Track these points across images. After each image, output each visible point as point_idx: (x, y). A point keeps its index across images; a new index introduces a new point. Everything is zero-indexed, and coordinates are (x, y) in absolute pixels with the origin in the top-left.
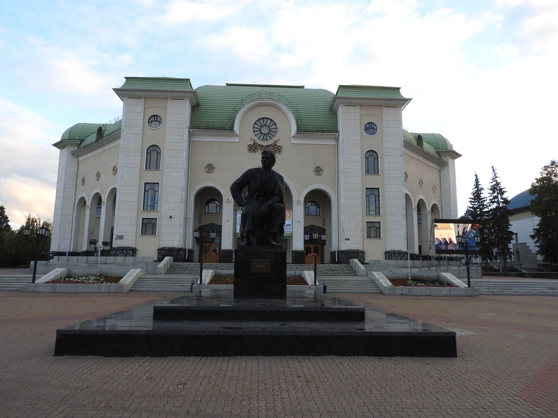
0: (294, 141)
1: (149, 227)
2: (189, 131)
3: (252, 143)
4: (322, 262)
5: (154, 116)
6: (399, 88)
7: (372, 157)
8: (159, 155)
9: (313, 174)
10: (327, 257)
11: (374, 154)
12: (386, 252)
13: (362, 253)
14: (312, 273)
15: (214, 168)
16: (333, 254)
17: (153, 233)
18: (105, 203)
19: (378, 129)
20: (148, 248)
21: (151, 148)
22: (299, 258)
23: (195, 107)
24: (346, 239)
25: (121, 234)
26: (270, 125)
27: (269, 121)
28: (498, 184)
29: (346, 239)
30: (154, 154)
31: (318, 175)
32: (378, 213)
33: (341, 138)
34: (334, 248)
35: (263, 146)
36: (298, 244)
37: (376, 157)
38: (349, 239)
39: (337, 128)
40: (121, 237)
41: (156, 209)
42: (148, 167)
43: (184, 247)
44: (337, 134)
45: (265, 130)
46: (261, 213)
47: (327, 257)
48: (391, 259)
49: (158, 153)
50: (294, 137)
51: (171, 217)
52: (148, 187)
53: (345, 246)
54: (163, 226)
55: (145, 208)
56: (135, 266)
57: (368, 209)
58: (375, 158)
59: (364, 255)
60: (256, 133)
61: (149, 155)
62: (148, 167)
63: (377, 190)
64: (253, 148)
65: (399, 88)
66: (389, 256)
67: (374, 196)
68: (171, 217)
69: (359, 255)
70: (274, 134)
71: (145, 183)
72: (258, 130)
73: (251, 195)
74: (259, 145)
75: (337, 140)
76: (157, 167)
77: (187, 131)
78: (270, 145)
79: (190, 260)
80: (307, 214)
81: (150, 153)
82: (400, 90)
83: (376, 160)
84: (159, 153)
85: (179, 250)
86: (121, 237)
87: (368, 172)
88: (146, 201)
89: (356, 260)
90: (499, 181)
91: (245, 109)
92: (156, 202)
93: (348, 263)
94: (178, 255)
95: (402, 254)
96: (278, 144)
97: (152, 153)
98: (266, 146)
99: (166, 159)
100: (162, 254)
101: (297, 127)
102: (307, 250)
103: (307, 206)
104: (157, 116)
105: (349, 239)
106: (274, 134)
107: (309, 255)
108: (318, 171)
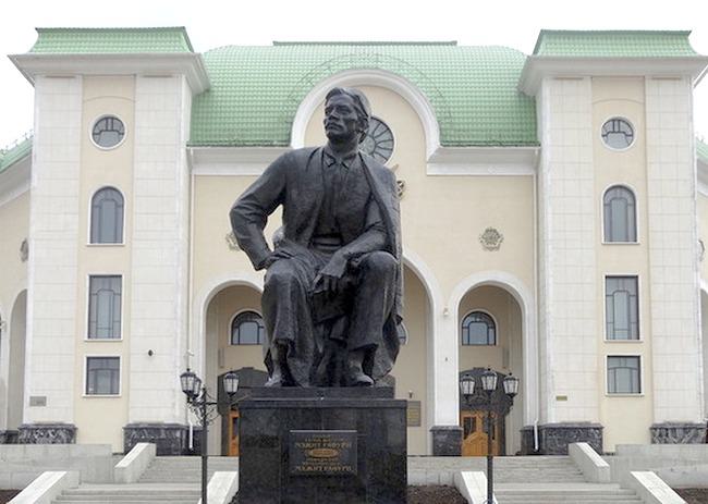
0: (433, 170)
1: (102, 374)
2: (188, 151)
4: (502, 453)
5: (106, 118)
6: (688, 33)
7: (622, 204)
10: (514, 440)
11: (625, 194)
12: (654, 428)
13: (595, 429)
14: (482, 477)
16: (528, 433)
19: (636, 133)
20: (101, 423)
21: (102, 195)
22: (448, 444)
23: (202, 97)
24: (558, 398)
25: (40, 394)
26: (377, 133)
29: (558, 398)
30: (109, 207)
31: (491, 249)
32: (634, 333)
33: (548, 155)
34: (531, 420)
36: (446, 411)
37: (630, 201)
38: (565, 398)
39: (536, 135)
40: (39, 402)
42: (96, 238)
43: (183, 423)
44: (537, 148)
46: (321, 282)
47: (514, 440)
48: (666, 442)
50: (432, 161)
51: (150, 353)
52: (98, 284)
53: (556, 416)
54: (132, 374)
57: (610, 326)
58: (627, 205)
59: (600, 434)
61: (97, 210)
62: (96, 238)
63: (633, 281)
65: (688, 33)
66: (660, 435)
67: (625, 295)
68: (150, 353)
69: (590, 433)
70: (385, 153)
71: (91, 277)
73: (293, 230)
75: (536, 163)
76: (117, 238)
77: (183, 151)
80: (466, 341)
82: (689, 37)
83: (630, 209)
84: (119, 206)
85: (172, 428)
86: (39, 402)
87: (610, 237)
88: (93, 319)
89: (585, 446)
91: (315, 96)
92: (116, 319)
93: (564, 452)
94: (168, 441)
95: (693, 431)
97: (105, 204)
99: (136, 217)
101: (441, 134)
102: (468, 425)
103: (466, 325)
104: (113, 118)
105: (565, 398)
106: (385, 153)
107: (471, 437)
108: (491, 238)
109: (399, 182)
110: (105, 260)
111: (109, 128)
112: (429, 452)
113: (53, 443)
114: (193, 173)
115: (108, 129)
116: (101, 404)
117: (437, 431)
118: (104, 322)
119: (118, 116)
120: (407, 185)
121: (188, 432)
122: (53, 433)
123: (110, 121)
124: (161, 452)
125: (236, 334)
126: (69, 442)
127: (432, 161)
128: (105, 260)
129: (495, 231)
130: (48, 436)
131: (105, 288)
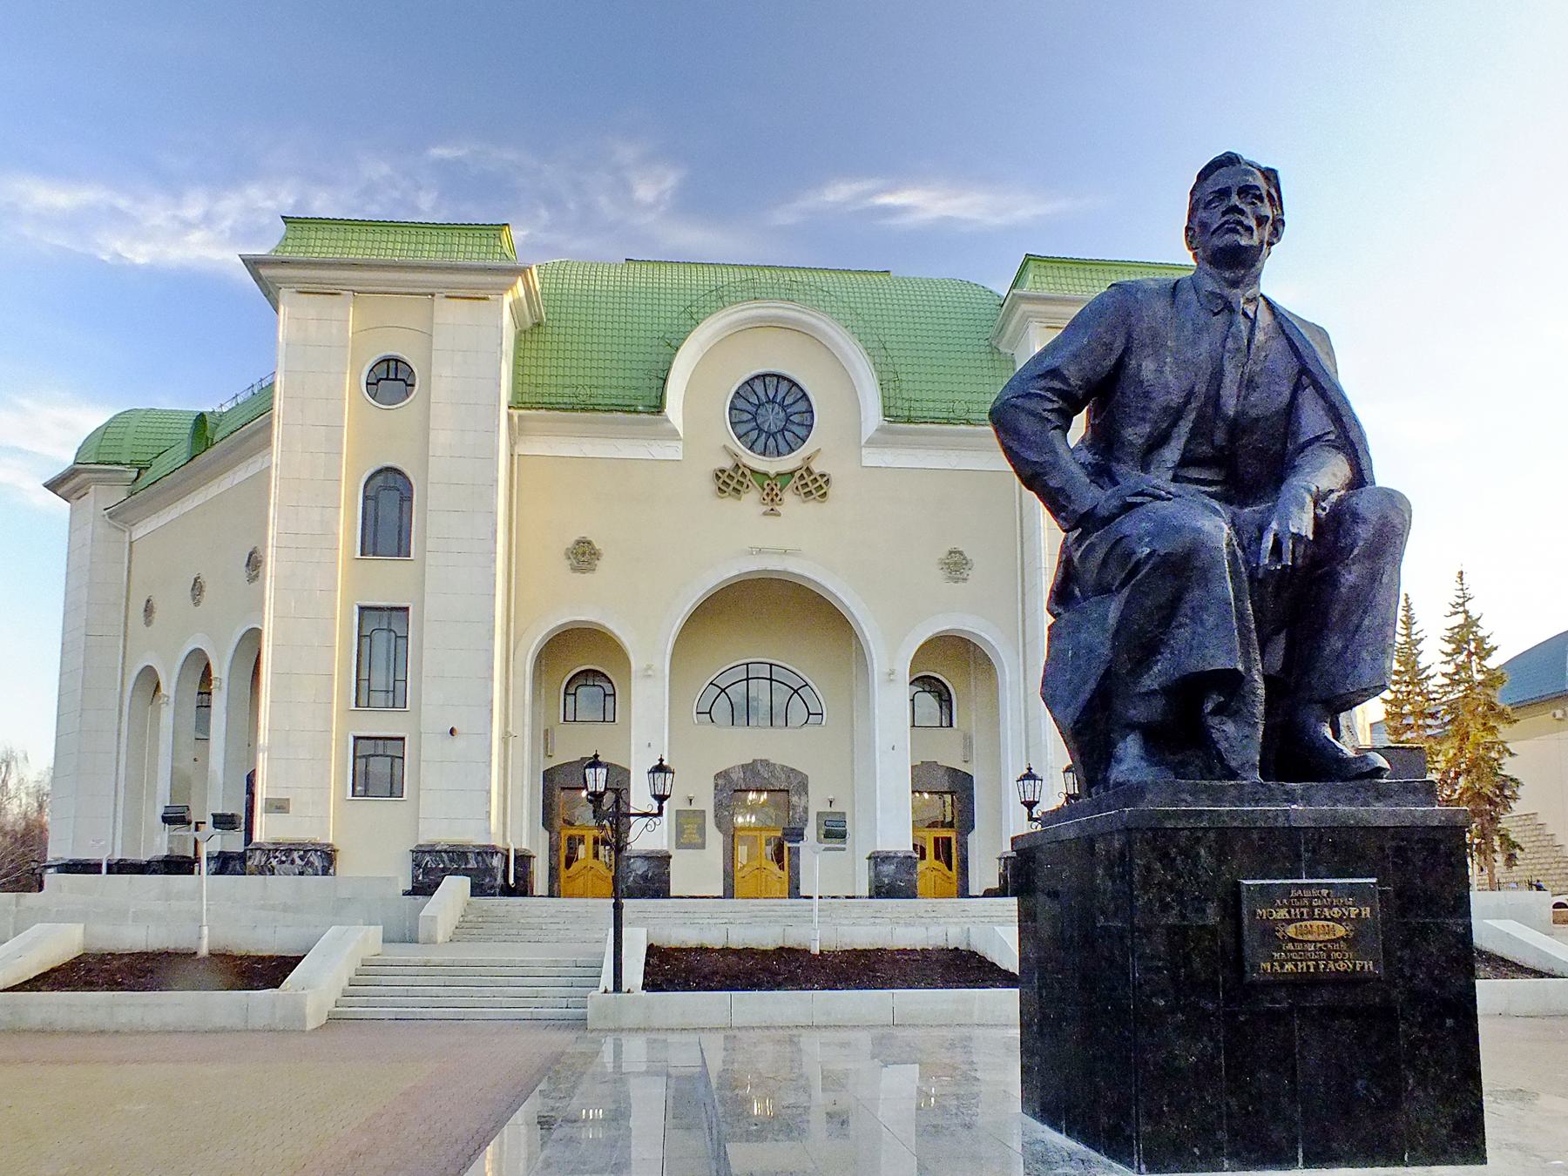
0: (871, 458)
1: (378, 768)
2: (510, 417)
3: (728, 464)
5: (387, 360)
8: (406, 504)
9: (939, 575)
15: (595, 554)
17: (394, 789)
18: (225, 685)
20: (376, 846)
21: (379, 479)
27: (784, 386)
28: (1470, 623)
35: (766, 475)
40: (278, 806)
41: (399, 703)
43: (499, 844)
45: (772, 418)
49: (402, 500)
50: (871, 443)
51: (452, 731)
52: (372, 623)
54: (428, 766)
55: (364, 701)
56: (340, 910)
60: (743, 429)
61: (371, 503)
64: (733, 484)
72: (746, 416)
74: (752, 471)
76: (401, 549)
78: (792, 473)
79: (522, 888)
81: (376, 499)
86: (278, 806)
88: (364, 675)
90: (1474, 614)
92: (400, 677)
96: (817, 468)
98: (778, 475)
99: (432, 518)
100: (427, 871)
104: (397, 361)
109: (822, 476)
110: (387, 582)
111: (392, 376)
112: (864, 890)
113: (301, 873)
114: (518, 450)
115: (391, 377)
116: (379, 809)
117: (877, 859)
118: (380, 679)
119: (406, 358)
120: (833, 480)
121: (507, 858)
122: (302, 858)
123: (392, 364)
124: (478, 890)
125: (570, 699)
126: (325, 872)
127: (871, 443)
128: (387, 582)
129: (961, 553)
130: (293, 862)
131: (383, 625)
